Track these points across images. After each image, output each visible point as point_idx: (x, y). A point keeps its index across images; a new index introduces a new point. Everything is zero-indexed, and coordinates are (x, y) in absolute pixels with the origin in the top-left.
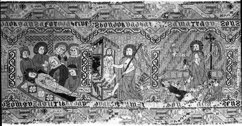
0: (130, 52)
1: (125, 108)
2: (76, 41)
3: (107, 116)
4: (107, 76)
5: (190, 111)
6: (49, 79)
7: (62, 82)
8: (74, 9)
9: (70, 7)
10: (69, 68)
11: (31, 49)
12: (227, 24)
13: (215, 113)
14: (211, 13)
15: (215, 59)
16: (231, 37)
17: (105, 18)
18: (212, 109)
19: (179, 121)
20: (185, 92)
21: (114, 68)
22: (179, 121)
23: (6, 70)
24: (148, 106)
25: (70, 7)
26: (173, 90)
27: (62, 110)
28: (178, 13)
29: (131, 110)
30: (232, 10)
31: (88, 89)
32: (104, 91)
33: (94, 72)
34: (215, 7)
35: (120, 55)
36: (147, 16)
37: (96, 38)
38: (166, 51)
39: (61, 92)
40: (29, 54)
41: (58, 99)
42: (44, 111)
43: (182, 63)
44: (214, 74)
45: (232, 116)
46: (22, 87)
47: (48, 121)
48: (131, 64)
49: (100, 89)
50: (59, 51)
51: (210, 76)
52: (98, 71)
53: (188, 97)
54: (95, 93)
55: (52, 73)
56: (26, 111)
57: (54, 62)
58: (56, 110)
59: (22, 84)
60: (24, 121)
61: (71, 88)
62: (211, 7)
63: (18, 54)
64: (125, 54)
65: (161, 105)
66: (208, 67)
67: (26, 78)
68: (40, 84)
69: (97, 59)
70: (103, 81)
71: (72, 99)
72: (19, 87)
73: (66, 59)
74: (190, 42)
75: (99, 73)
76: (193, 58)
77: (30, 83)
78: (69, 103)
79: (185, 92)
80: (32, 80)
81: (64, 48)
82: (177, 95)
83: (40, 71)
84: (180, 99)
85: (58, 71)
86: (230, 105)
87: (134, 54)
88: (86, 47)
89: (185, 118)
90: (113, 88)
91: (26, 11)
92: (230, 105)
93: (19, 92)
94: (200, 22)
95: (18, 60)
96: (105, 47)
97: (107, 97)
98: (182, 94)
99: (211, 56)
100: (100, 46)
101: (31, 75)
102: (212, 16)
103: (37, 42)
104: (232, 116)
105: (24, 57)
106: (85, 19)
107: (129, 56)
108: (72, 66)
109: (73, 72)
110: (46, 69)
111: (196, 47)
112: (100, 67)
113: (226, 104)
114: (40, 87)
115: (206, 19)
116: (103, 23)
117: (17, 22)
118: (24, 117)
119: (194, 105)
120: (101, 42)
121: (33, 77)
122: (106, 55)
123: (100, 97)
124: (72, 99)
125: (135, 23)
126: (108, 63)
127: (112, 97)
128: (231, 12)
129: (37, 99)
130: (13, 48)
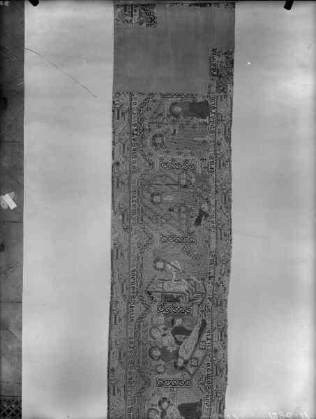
0: (160, 265)
1: (215, 271)
2: (148, 319)
3: (221, 288)
4: (183, 288)
5: (218, 206)
6: (184, 346)
7: (188, 333)
8: (118, 319)
9: (115, 322)
10: (175, 326)
11: (154, 363)
12: (134, 167)
13: (221, 181)
14: (123, 183)
15: (169, 181)
16: (147, 164)
17: (127, 289)
18: (218, 184)
19: (227, 217)
20: (200, 210)
21: (175, 281)
22: (227, 217)
23: (175, 389)
24: (213, 247)
25: (115, 322)
26: (198, 222)
27: (214, 333)
28: (123, 216)
29: (216, 264)
30: (121, 162)
31: (195, 307)
32: (198, 290)
33: (179, 301)
34: (118, 179)
35: (162, 275)
36: (125, 247)
37: (146, 298)
38: (160, 228)
39: (197, 333)
40: (160, 365)
41: (204, 338)
42: (216, 351)
43: (172, 213)
44: (183, 182)
45: (224, 165)
46: (192, 372)
47: (225, 347)
48: (172, 263)
49: (195, 295)
50: (157, 335)
51: (185, 186)
52: (178, 297)
53: (205, 207)
54: (199, 301)
55: (179, 343)
56: (215, 371)
57: (168, 341)
58: (214, 339)
59: (189, 373)
60: (224, 371)
61: (193, 325)
62: (118, 183)
63: (161, 376)
64: (162, 270)
65: (213, 235)
66: (176, 187)
67: (182, 368)
68: (189, 354)
69: (166, 297)
70: (188, 292)
71: (204, 324)
72: (192, 376)
73: (165, 329)
74: (151, 206)
75: (181, 296)
76: (167, 202)
77: (188, 365)
78: (207, 326)
79: (200, 210)
80: (186, 362)
81: (154, 331)
82: (203, 218)
83: (176, 354)
84: (207, 215)
85: (177, 336)
86: (213, 166)
87: (163, 261)
88: (154, 307)
89: (225, 211)
90: (195, 282)
91: (117, 368)
92: (213, 166)
93: (196, 376)
94: (132, 194)
95: (165, 376)
96: (154, 289)
97: (203, 288)
98: (202, 214)
99: (167, 185)
100: (153, 293)
101: (180, 363)
102: (126, 182)
103: (148, 357)
104: (224, 165)
105: (162, 370)
106: (127, 309)
107: (165, 265)
108: (173, 322)
109: (178, 322)
110: (175, 349)
111: (157, 199)
112: (174, 295)
113: (212, 171)
114: (192, 354)
115: (129, 188)
116: (132, 291)
117: (129, 376)
118: (221, 371)
119: (212, 201)
120: (149, 293)
121: (182, 361)
122: (162, 288)
123: (203, 294)
124: (204, 324)
125: (132, 259)
126: (171, 287)
127: (203, 284)
128: (123, 163)
129: (204, 358)
130: (153, 382)
